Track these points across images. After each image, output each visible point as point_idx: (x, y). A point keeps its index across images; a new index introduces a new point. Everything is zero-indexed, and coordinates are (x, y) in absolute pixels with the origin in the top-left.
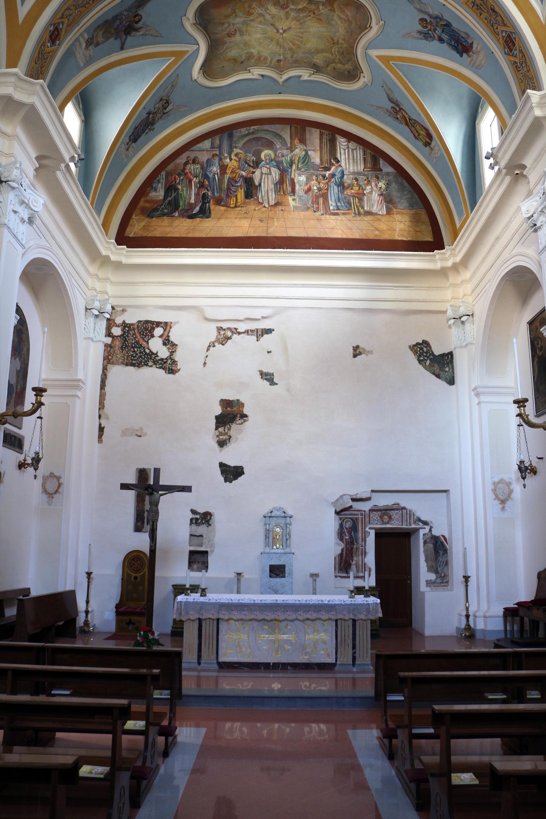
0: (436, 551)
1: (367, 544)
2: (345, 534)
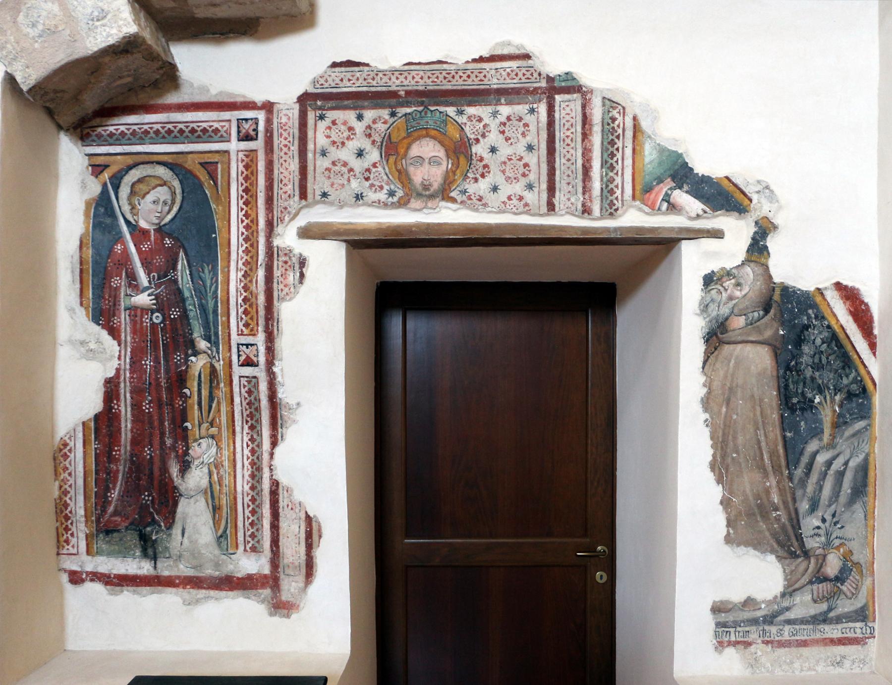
0: (794, 403)
1: (283, 344)
2: (132, 277)
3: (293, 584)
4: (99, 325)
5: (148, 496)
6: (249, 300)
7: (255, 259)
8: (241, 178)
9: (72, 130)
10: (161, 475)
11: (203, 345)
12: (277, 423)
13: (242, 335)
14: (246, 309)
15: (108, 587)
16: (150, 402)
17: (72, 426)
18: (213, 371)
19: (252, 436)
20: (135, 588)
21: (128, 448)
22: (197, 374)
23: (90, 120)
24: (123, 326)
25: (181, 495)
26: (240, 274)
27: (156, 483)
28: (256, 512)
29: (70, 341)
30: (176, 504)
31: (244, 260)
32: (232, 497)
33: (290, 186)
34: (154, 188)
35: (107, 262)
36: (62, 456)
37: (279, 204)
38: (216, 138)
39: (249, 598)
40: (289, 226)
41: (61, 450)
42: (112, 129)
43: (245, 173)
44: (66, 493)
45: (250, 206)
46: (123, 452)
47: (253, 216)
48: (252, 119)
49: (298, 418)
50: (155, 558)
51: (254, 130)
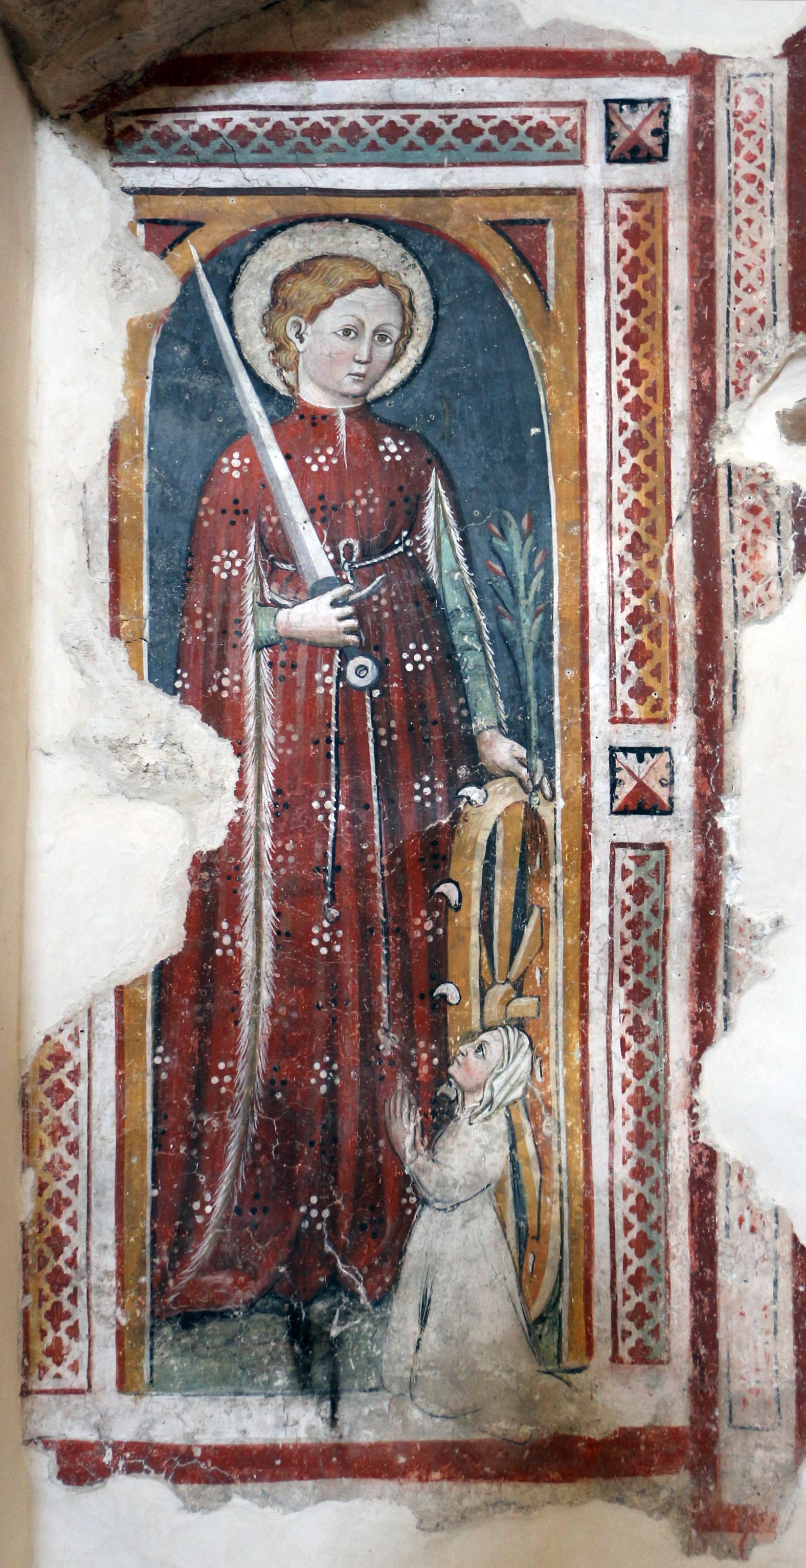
1: (745, 746)
2: (278, 551)
3: (760, 1453)
4: (174, 691)
5: (320, 1207)
6: (649, 619)
7: (661, 500)
8: (616, 269)
9: (75, 117)
10: (363, 1144)
11: (502, 750)
12: (712, 978)
13: (625, 720)
14: (639, 646)
15: (183, 1487)
16: (336, 924)
17: (81, 999)
18: (533, 831)
19: (637, 1019)
20: (266, 1486)
21: (261, 1063)
22: (483, 838)
23: (134, 91)
24: (251, 696)
25: (424, 1202)
26: (620, 544)
27: (345, 1168)
28: (651, 1244)
29: (78, 743)
30: (405, 1228)
31: (628, 503)
32: (578, 1202)
33: (764, 293)
34: (344, 292)
35: (199, 506)
36: (48, 1093)
37: (729, 345)
38: (540, 152)
39: (621, 1500)
40: (755, 408)
41: (45, 1074)
42: (206, 119)
43: (630, 252)
44: (57, 1205)
45: (644, 348)
46: (242, 1075)
47: (655, 374)
48: (650, 102)
49: (769, 962)
50: (333, 1394)
51: (656, 132)
